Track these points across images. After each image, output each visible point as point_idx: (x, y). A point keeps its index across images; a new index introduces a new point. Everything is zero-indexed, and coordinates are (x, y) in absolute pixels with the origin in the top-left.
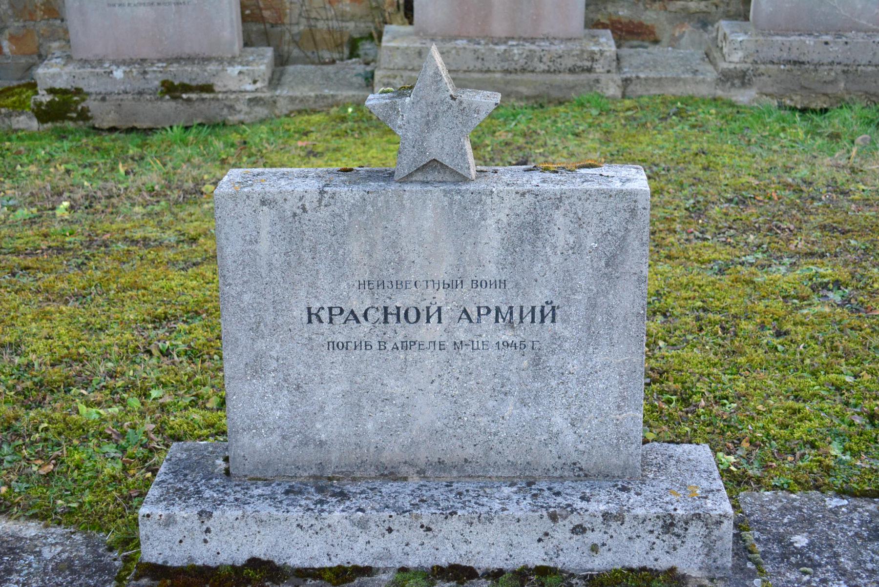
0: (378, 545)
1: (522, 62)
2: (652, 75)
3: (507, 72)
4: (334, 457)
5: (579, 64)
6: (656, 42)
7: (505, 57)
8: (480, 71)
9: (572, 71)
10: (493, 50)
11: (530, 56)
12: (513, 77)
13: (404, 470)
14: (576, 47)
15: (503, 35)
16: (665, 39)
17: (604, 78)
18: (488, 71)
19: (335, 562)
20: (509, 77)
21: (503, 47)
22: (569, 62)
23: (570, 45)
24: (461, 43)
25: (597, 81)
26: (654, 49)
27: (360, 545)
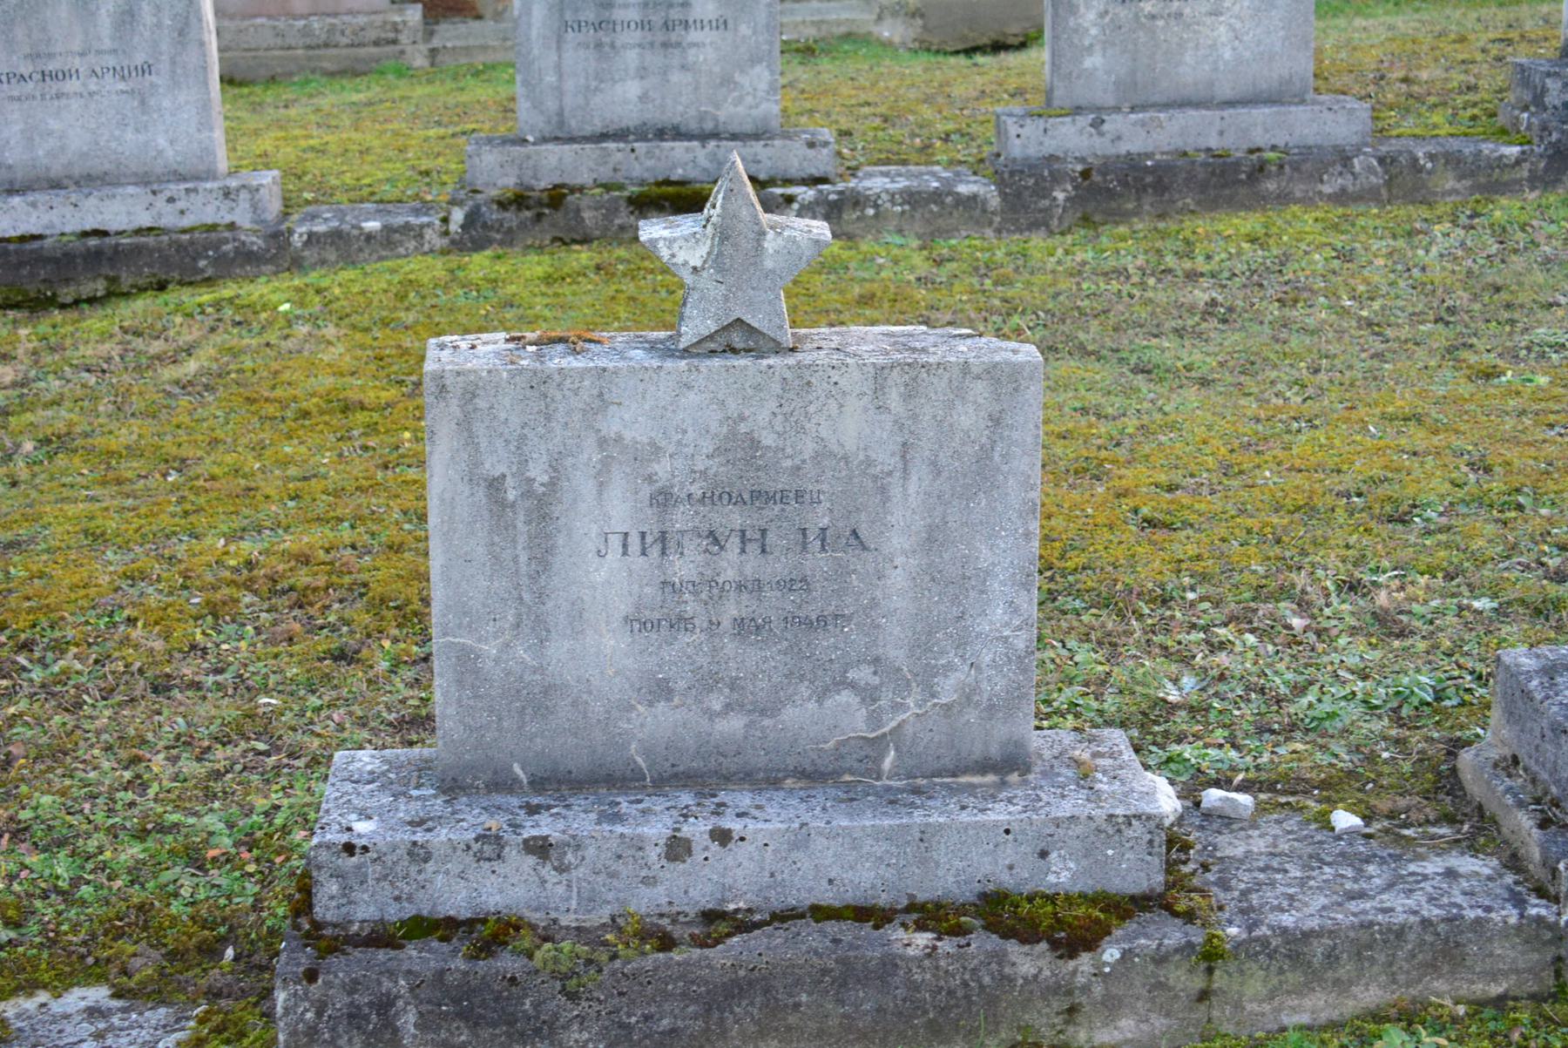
0: (46, 218)
1: (324, 36)
2: (459, 43)
3: (309, 47)
4: (19, 176)
5: (383, 35)
6: (479, 17)
7: (306, 32)
8: (282, 48)
9: (376, 43)
10: (292, 26)
11: (332, 29)
12: (317, 52)
13: (66, 182)
14: (378, 19)
15: (306, 11)
16: (488, 13)
17: (409, 49)
18: (289, 48)
19: (19, 233)
20: (311, 53)
21: (303, 22)
22: (372, 35)
23: (373, 17)
24: (259, 21)
25: (402, 52)
26: (475, 25)
27: (33, 219)
